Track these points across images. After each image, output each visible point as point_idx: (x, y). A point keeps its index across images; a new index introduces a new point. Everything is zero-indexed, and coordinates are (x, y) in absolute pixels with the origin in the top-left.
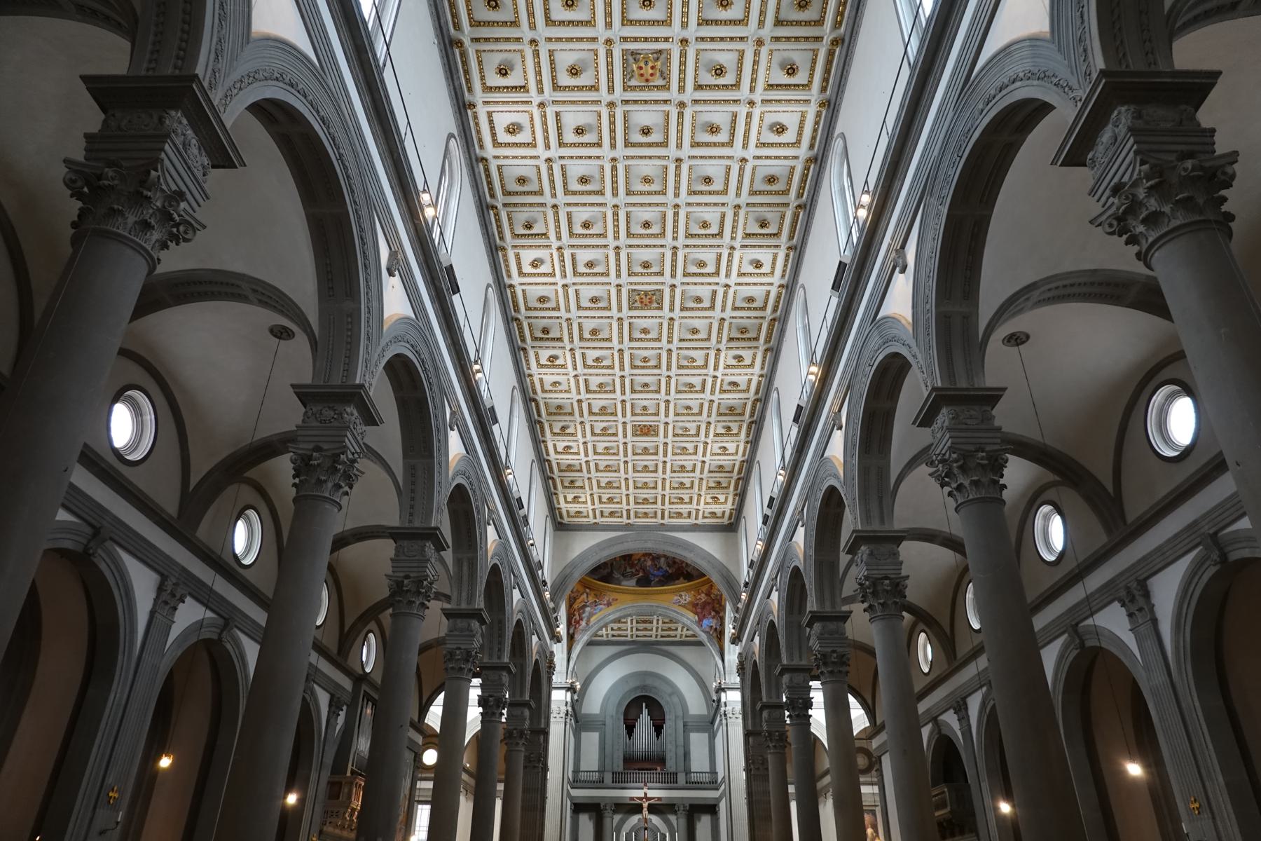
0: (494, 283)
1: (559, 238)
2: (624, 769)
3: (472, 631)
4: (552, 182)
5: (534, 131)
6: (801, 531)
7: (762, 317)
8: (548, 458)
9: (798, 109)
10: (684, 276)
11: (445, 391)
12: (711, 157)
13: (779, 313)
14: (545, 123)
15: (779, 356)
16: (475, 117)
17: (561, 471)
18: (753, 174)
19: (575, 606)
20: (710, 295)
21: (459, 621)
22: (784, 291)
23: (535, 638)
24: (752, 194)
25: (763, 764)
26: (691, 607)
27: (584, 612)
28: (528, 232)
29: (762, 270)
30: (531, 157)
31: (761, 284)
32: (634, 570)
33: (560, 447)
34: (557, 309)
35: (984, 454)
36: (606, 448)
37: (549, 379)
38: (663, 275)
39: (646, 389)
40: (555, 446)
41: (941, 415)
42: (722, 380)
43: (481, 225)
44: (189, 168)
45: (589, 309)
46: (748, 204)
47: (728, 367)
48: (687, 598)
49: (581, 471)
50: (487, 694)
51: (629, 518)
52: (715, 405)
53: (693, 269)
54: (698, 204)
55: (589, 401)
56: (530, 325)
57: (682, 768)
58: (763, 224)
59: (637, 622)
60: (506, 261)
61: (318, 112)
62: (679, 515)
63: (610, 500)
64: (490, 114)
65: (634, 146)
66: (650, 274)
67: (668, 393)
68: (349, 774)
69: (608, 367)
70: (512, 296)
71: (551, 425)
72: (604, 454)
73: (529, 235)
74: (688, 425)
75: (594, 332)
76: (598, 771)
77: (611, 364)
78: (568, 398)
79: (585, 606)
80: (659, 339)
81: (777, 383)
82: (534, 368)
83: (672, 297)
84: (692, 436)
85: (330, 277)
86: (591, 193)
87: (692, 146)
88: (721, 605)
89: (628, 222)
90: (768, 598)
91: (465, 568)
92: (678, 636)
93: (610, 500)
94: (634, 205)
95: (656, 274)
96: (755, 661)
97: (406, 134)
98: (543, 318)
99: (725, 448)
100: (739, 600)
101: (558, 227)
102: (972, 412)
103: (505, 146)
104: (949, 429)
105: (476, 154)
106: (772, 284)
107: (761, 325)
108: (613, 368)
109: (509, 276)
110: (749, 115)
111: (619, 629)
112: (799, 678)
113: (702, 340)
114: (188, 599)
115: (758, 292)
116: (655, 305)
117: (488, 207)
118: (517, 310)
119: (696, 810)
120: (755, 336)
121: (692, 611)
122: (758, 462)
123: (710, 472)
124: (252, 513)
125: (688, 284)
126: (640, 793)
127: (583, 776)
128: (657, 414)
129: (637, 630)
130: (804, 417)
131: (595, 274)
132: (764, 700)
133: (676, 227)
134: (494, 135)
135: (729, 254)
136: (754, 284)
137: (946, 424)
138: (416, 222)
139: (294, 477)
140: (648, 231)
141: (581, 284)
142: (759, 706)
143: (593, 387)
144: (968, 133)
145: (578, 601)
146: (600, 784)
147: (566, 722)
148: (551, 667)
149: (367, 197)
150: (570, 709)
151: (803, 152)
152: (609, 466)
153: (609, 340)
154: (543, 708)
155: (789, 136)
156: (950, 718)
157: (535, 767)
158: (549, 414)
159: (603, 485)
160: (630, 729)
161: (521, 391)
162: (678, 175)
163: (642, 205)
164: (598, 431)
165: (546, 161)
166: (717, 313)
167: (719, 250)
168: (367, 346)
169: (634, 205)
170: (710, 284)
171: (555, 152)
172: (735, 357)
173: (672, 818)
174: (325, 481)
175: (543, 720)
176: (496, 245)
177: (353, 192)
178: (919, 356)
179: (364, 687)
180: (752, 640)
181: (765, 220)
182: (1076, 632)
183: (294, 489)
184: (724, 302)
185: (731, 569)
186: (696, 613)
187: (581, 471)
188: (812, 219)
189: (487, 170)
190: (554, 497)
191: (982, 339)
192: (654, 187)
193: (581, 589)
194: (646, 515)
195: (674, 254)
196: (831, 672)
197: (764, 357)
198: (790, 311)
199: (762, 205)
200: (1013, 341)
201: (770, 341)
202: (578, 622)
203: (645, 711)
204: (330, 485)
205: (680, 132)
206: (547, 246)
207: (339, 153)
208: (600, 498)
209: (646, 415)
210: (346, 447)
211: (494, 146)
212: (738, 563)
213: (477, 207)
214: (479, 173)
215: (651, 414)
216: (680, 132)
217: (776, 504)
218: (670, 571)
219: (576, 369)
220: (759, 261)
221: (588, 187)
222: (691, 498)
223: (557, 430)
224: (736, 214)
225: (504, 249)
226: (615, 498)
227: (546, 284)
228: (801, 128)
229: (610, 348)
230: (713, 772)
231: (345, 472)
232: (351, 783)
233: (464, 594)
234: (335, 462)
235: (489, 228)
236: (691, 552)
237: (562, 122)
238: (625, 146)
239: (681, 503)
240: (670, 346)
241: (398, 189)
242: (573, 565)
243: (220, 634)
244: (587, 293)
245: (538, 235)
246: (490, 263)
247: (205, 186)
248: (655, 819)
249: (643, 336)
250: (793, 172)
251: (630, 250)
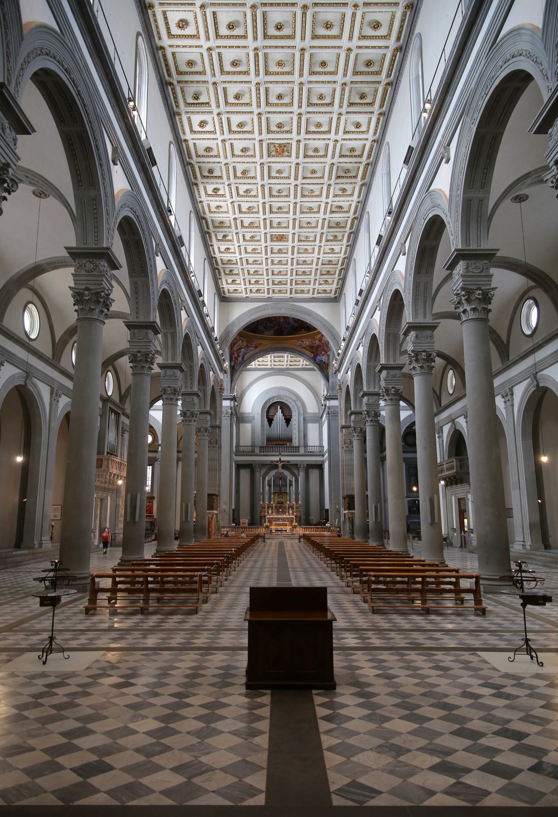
0: (174, 139)
1: (218, 106)
3: (176, 377)
4: (212, 65)
5: (197, 26)
6: (378, 313)
7: (360, 162)
8: (213, 256)
9: (390, 10)
10: (306, 133)
11: (152, 233)
12: (326, 47)
13: (371, 159)
14: (205, 20)
15: (371, 189)
16: (154, 15)
17: (223, 264)
18: (356, 59)
19: (235, 348)
20: (324, 146)
21: (168, 370)
22: (375, 144)
23: (211, 373)
24: (355, 75)
25: (350, 444)
27: (240, 352)
28: (196, 102)
29: (362, 129)
30: (196, 47)
31: (360, 139)
32: (272, 325)
33: (223, 249)
34: (218, 156)
35: (480, 292)
36: (254, 249)
37: (213, 205)
38: (291, 132)
39: (280, 211)
40: (219, 248)
41: (458, 266)
42: (332, 205)
43: (163, 98)
44: (8, 145)
45: (241, 156)
46: (352, 82)
47: (335, 196)
48: (307, 342)
49: (237, 264)
50: (185, 410)
51: (269, 293)
52: (326, 222)
53: (312, 128)
54: (316, 82)
55: (242, 219)
56: (200, 168)
57: (302, 444)
58: (362, 97)
59: (274, 357)
60: (181, 122)
61: (63, 66)
62: (302, 291)
63: (257, 282)
64: (164, 13)
65: (270, 38)
66: (282, 132)
67: (295, 213)
68: (106, 454)
69: (254, 196)
70: (186, 147)
71: (216, 235)
72: (252, 253)
73: (197, 104)
74: (308, 234)
75: (244, 172)
76: (251, 446)
77: (256, 194)
78: (228, 217)
79: (241, 348)
80: (288, 178)
81: (369, 208)
82: (204, 198)
83: (298, 148)
84: (311, 241)
85: (79, 179)
86: (240, 73)
87: (313, 38)
88: (328, 347)
89: (267, 95)
90: (357, 350)
91: (169, 339)
92: (301, 365)
93: (257, 282)
94: (271, 82)
95: (287, 132)
96: (348, 386)
97: (97, 11)
98: (208, 163)
99: (333, 249)
100: (340, 349)
101: (217, 98)
102: (478, 264)
103: (177, 38)
104: (463, 276)
105: (156, 44)
106: (367, 139)
107: (359, 167)
108: (258, 197)
109: (184, 133)
110: (354, 15)
111: (263, 361)
112: (373, 399)
113: (319, 178)
114: (6, 364)
115: (357, 144)
116: (286, 154)
117: (166, 83)
118: (190, 157)
119: (310, 467)
120: (354, 175)
121: (310, 351)
122: (355, 259)
123: (323, 264)
124: (30, 306)
125: (309, 139)
126: (277, 459)
127: (241, 449)
128: (287, 227)
129: (274, 361)
130: (383, 242)
131: (244, 132)
132: (352, 409)
133: (300, 99)
134: (168, 29)
135: (338, 118)
136: (355, 139)
137: (461, 272)
138: (126, 121)
139: (74, 305)
140: (281, 102)
141: (235, 139)
142: (349, 412)
143: (244, 209)
144: (493, 79)
145: (237, 344)
146: (252, 453)
147: (231, 419)
148: (222, 389)
149: (97, 115)
150: (233, 411)
151: (392, 43)
152: (255, 261)
153: (254, 178)
154: (218, 413)
155: (383, 31)
156: (461, 421)
157: (214, 447)
158: (215, 227)
159: (251, 272)
160: (270, 421)
161: (195, 214)
162: (302, 61)
163: (277, 82)
164: (247, 238)
165: (207, 50)
166: (329, 160)
167: (331, 116)
168: (108, 219)
169: (271, 82)
170: (324, 139)
171: (213, 43)
172: (340, 190)
173: (296, 471)
174: (94, 309)
175: (218, 420)
176: (173, 111)
177: (88, 115)
178: (451, 224)
179: (109, 405)
180: (347, 373)
181: (364, 93)
182: (535, 378)
183: (76, 313)
184: (334, 152)
185: (335, 326)
186: (312, 352)
187: (237, 264)
188: (397, 94)
189: (164, 56)
190: (219, 281)
191: (490, 214)
192: (285, 69)
193: (238, 338)
194: (280, 291)
195: (300, 119)
196: (391, 399)
197: (361, 190)
198: (379, 158)
199: (362, 82)
200: (518, 200)
201: (365, 179)
202: (236, 358)
203: (280, 411)
204: (97, 311)
205: (304, 28)
206: (210, 112)
207: (78, 90)
208: (250, 281)
209: (280, 228)
210: (104, 288)
211: (169, 37)
212: (339, 322)
213: (159, 85)
214: (159, 58)
215: (283, 227)
216: (304, 28)
217: (364, 294)
218: (296, 325)
219: (232, 198)
220: (359, 123)
221: (239, 69)
222: (310, 281)
223: (220, 237)
224: (343, 90)
225: (179, 114)
226: (259, 281)
227: (210, 139)
228: (391, 24)
229: (255, 184)
230: (322, 446)
231: (104, 302)
232: (108, 459)
233: (170, 354)
234: (98, 297)
235: (168, 99)
236: (310, 315)
237: (218, 19)
238: (264, 39)
239: (304, 284)
240: (296, 182)
241: (113, 101)
242: (233, 324)
243: (25, 382)
244: (238, 146)
245: (203, 103)
246: (170, 125)
247: (17, 151)
248: (286, 473)
249: (278, 175)
250: (385, 58)
251: (268, 115)
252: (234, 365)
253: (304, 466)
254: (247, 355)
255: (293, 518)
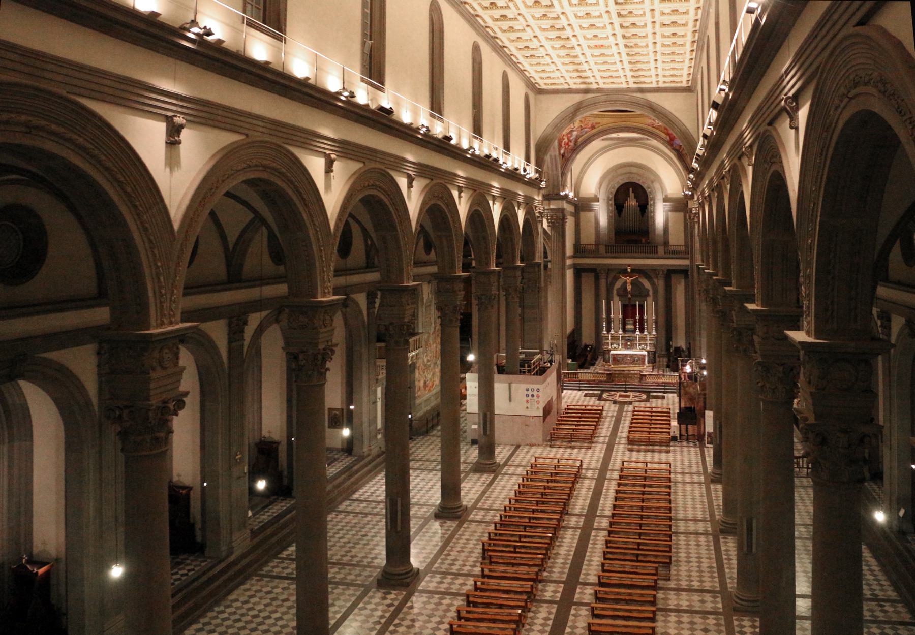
2: (616, 243)
27: (571, 136)
79: (572, 131)
119: (670, 273)
146: (595, 253)
203: (632, 195)
252: (564, 153)
253: (663, 271)
254: (581, 139)
255: (644, 355)
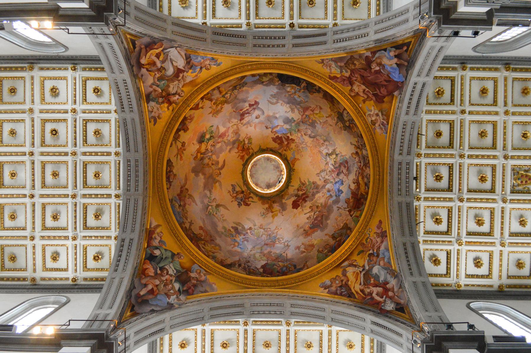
19: (356, 287)
26: (385, 106)
27: (377, 277)
79: (367, 275)
121: (391, 102)
186: (391, 94)
202: (386, 290)
